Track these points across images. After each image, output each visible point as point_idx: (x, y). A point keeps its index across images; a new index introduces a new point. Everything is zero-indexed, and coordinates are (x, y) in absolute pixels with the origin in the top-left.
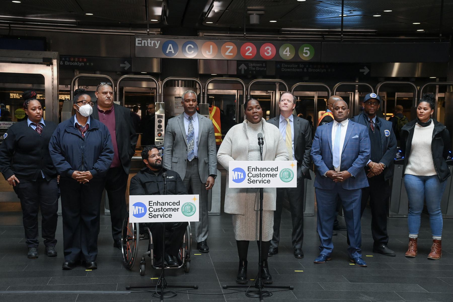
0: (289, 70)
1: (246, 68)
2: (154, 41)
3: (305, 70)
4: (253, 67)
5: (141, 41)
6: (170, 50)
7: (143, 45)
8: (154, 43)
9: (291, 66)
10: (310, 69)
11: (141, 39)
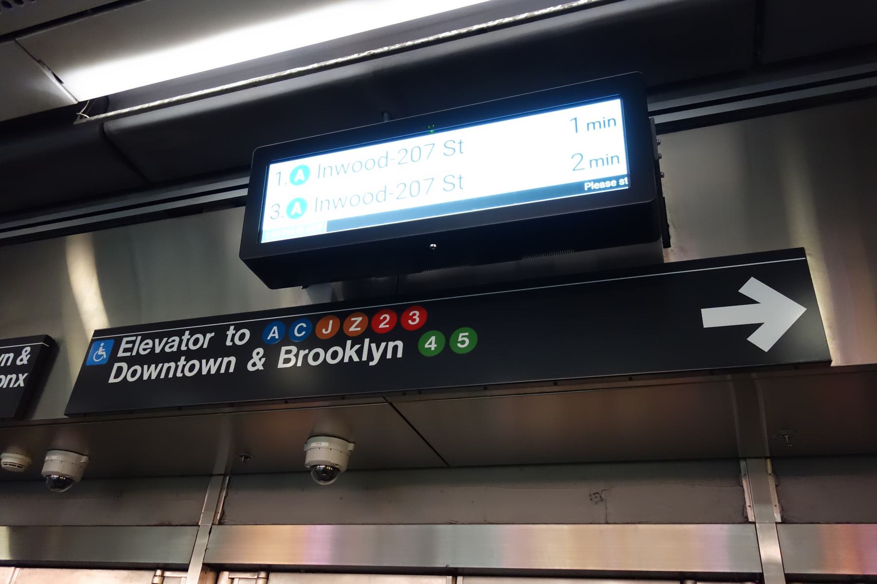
0: (151, 372)
3: (257, 361)
9: (173, 344)
10: (288, 352)
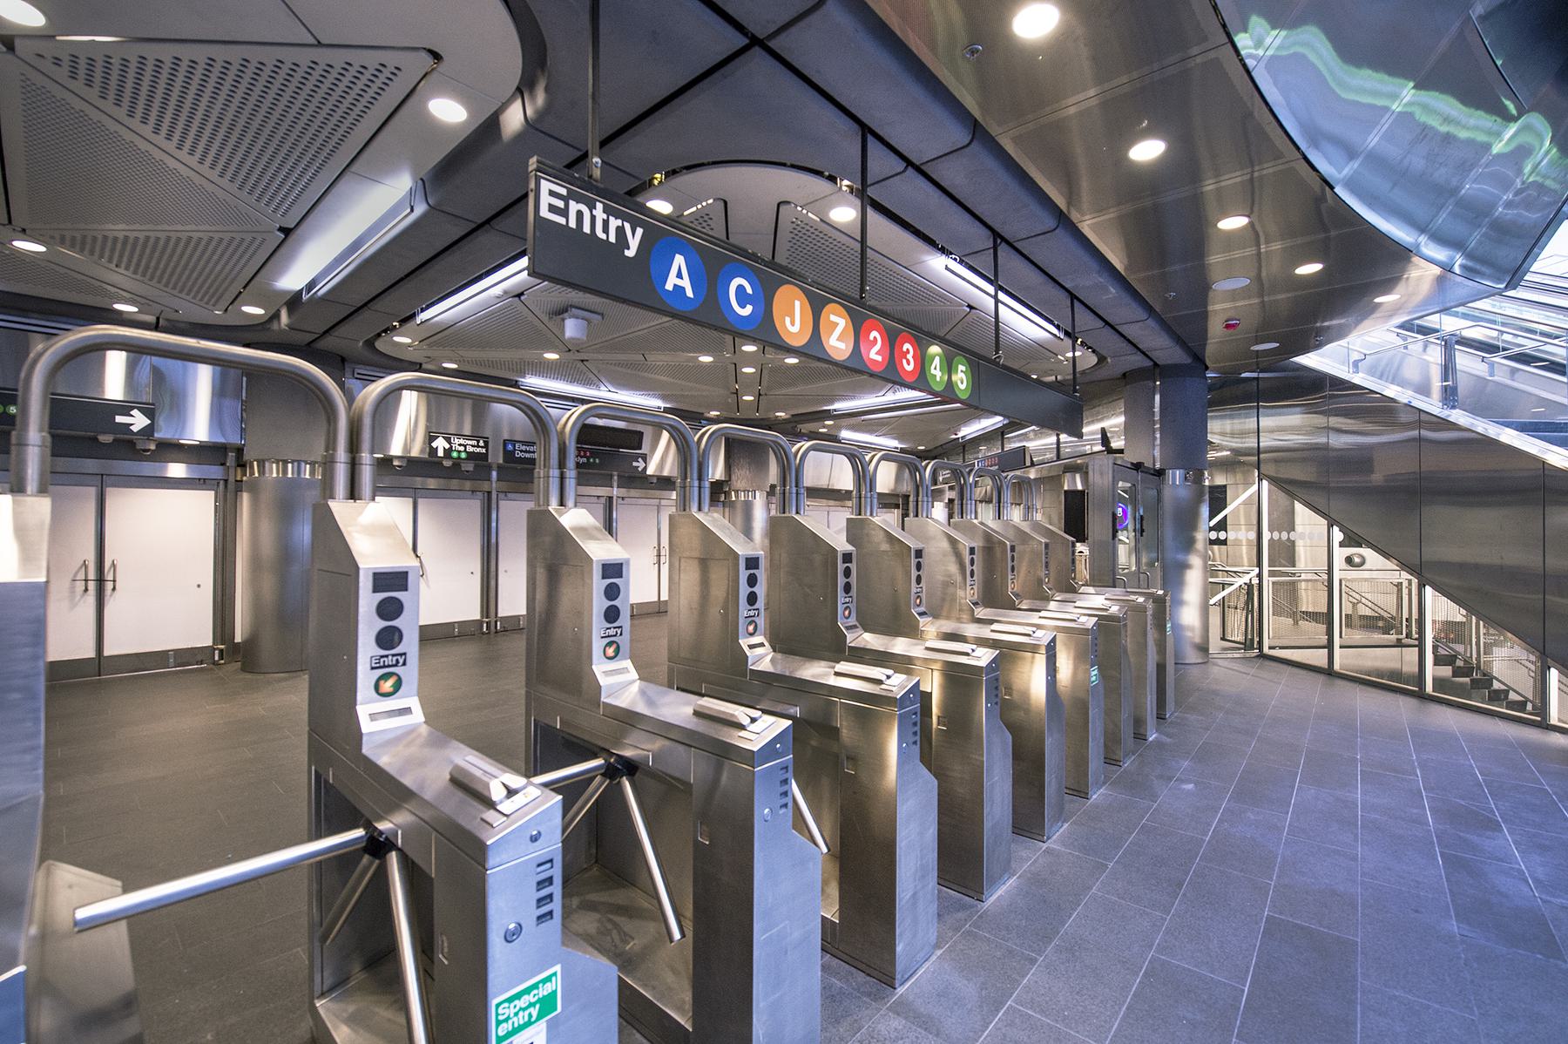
1: (447, 446)
2: (619, 222)
4: (460, 445)
5: (565, 199)
6: (679, 282)
7: (573, 224)
8: (621, 231)
11: (564, 192)
